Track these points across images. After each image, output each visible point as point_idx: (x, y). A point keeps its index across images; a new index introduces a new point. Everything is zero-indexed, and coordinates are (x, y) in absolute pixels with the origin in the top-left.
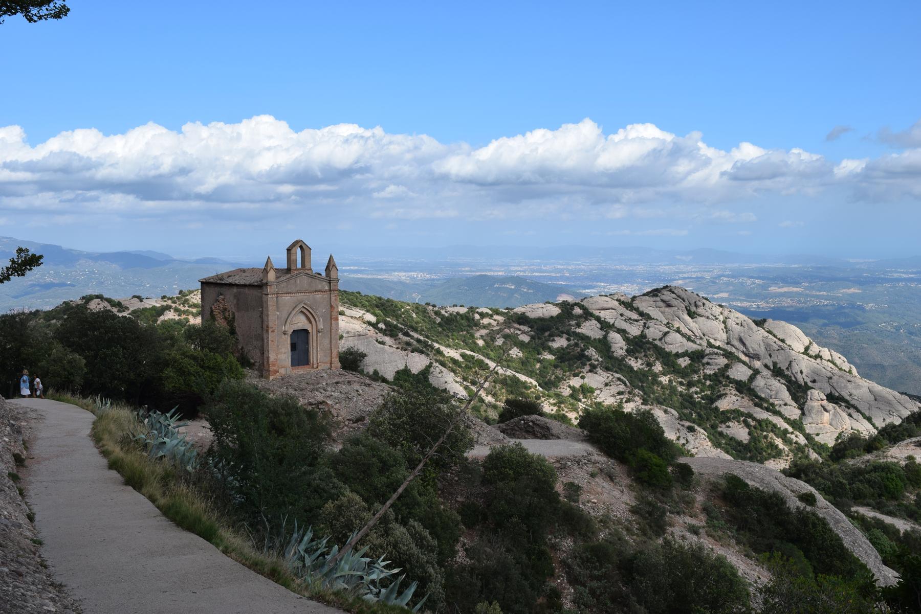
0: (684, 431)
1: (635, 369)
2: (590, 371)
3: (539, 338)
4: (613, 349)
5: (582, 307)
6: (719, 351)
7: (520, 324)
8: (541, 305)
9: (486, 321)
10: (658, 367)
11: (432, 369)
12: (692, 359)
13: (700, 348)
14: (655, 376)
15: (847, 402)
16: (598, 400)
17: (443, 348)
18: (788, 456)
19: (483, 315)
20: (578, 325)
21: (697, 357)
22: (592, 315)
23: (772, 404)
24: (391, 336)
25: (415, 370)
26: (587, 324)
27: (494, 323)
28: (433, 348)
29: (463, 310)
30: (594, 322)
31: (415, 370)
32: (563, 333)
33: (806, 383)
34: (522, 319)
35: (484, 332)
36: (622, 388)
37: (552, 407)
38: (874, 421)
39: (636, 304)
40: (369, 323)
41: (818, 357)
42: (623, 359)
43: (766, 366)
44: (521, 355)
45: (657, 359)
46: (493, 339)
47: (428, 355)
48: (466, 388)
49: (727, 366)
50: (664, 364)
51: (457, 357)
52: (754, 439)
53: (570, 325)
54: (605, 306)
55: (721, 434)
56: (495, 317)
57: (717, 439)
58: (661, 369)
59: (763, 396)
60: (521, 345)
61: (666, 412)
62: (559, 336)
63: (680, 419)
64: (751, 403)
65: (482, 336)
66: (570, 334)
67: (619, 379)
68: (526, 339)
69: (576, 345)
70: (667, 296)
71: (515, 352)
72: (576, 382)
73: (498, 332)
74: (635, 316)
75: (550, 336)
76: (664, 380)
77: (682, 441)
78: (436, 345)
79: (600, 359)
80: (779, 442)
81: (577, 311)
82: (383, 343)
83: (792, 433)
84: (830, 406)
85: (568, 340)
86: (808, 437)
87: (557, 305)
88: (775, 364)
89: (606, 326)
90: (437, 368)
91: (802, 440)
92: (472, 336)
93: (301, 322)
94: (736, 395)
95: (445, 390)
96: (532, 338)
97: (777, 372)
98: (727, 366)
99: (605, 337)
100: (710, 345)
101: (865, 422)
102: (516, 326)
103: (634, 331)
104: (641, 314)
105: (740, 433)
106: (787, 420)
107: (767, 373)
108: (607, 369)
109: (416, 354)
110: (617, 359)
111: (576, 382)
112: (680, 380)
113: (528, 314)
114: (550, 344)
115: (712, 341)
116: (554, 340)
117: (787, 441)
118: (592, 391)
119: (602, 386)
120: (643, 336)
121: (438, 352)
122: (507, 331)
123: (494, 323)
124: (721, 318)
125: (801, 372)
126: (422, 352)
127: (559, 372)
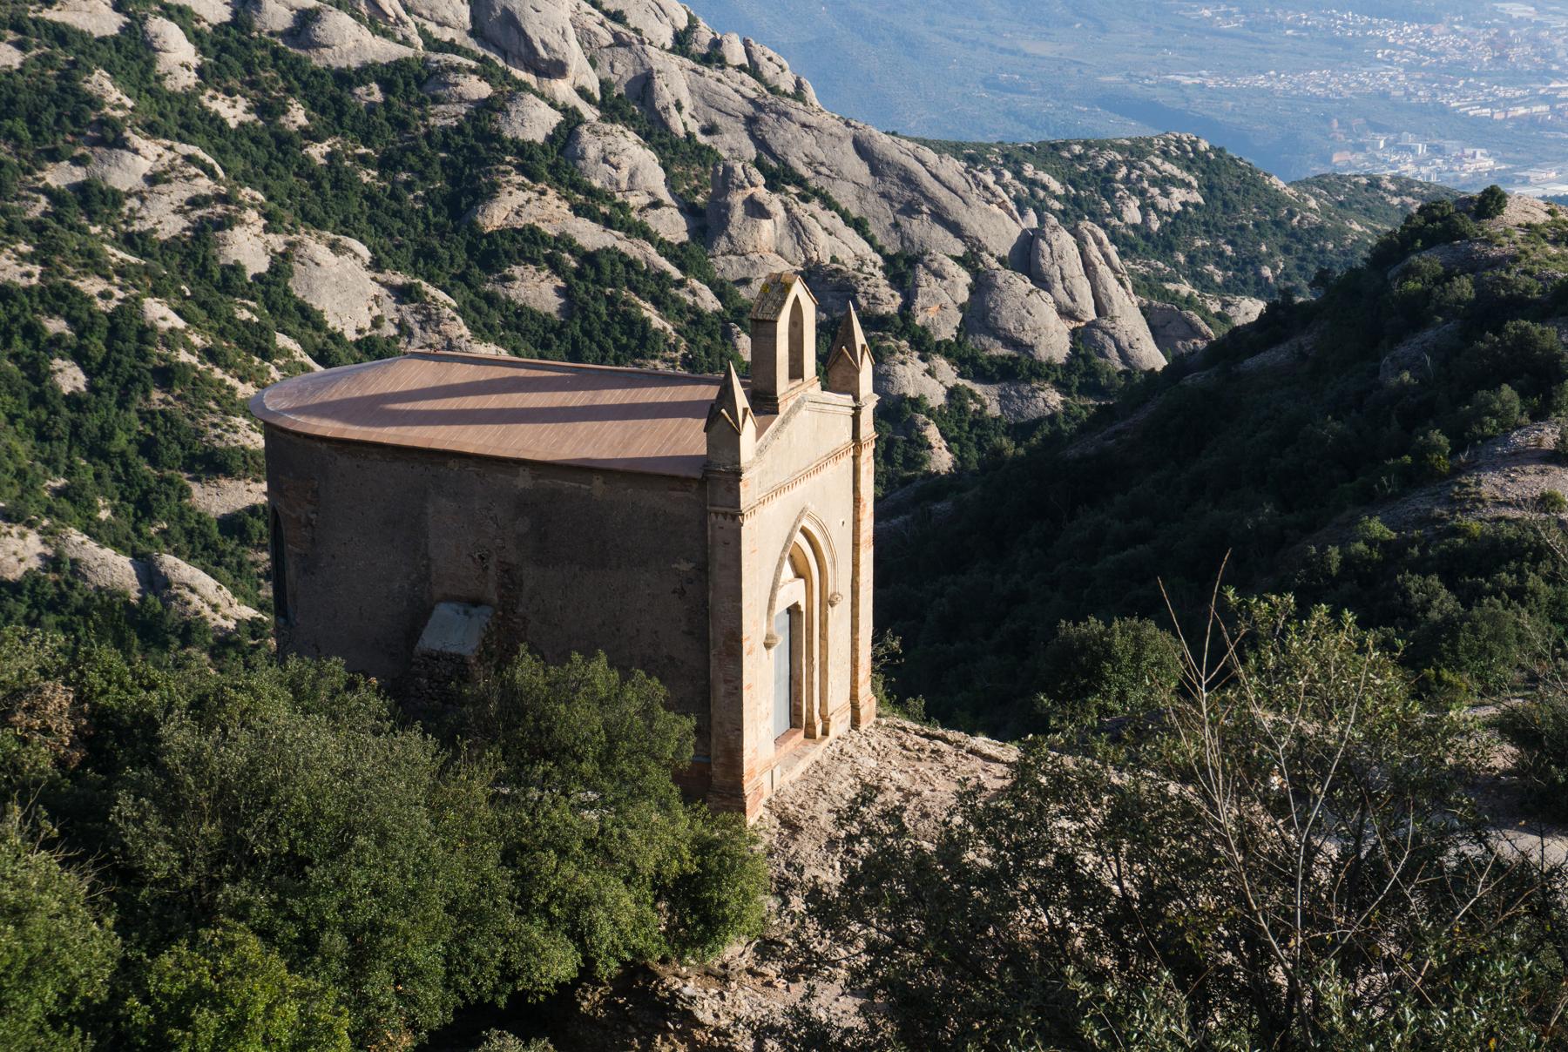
1: (233, 124)
4: (161, 68)
6: (465, 61)
10: (297, 116)
12: (387, 87)
13: (407, 52)
14: (284, 141)
15: (800, 182)
16: (137, 226)
18: (675, 348)
23: (623, 207)
33: (690, 136)
37: (28, 267)
38: (873, 230)
43: (582, 92)
45: (290, 91)
50: (312, 105)
55: (491, 299)
58: (302, 120)
59: (597, 184)
61: (334, 247)
63: (376, 265)
64: (565, 206)
67: (189, 159)
69: (45, 61)
79: (129, 103)
83: (680, 284)
84: (774, 203)
85: (21, 46)
86: (721, 290)
88: (605, 85)
91: (709, 302)
93: (793, 591)
94: (522, 187)
97: (611, 108)
100: (433, 44)
101: (849, 234)
105: (536, 290)
106: (663, 247)
107: (590, 113)
108: (152, 130)
110: (172, 97)
112: (363, 150)
115: (431, 27)
118: (115, 198)
119: (143, 185)
125: (679, 106)
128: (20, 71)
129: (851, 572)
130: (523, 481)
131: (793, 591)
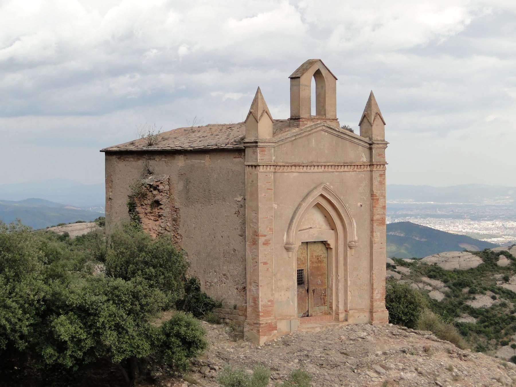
3: (456, 296)
5: (509, 256)
7: (430, 277)
20: (506, 279)
32: (485, 289)
34: (434, 272)
53: (495, 280)
56: (399, 268)
62: (482, 293)
68: (438, 296)
69: (504, 305)
81: (503, 261)
85: (494, 298)
87: (475, 254)
96: (447, 295)
102: (425, 279)
113: (441, 265)
114: (469, 303)
116: (474, 298)
123: (398, 276)
128: (492, 308)
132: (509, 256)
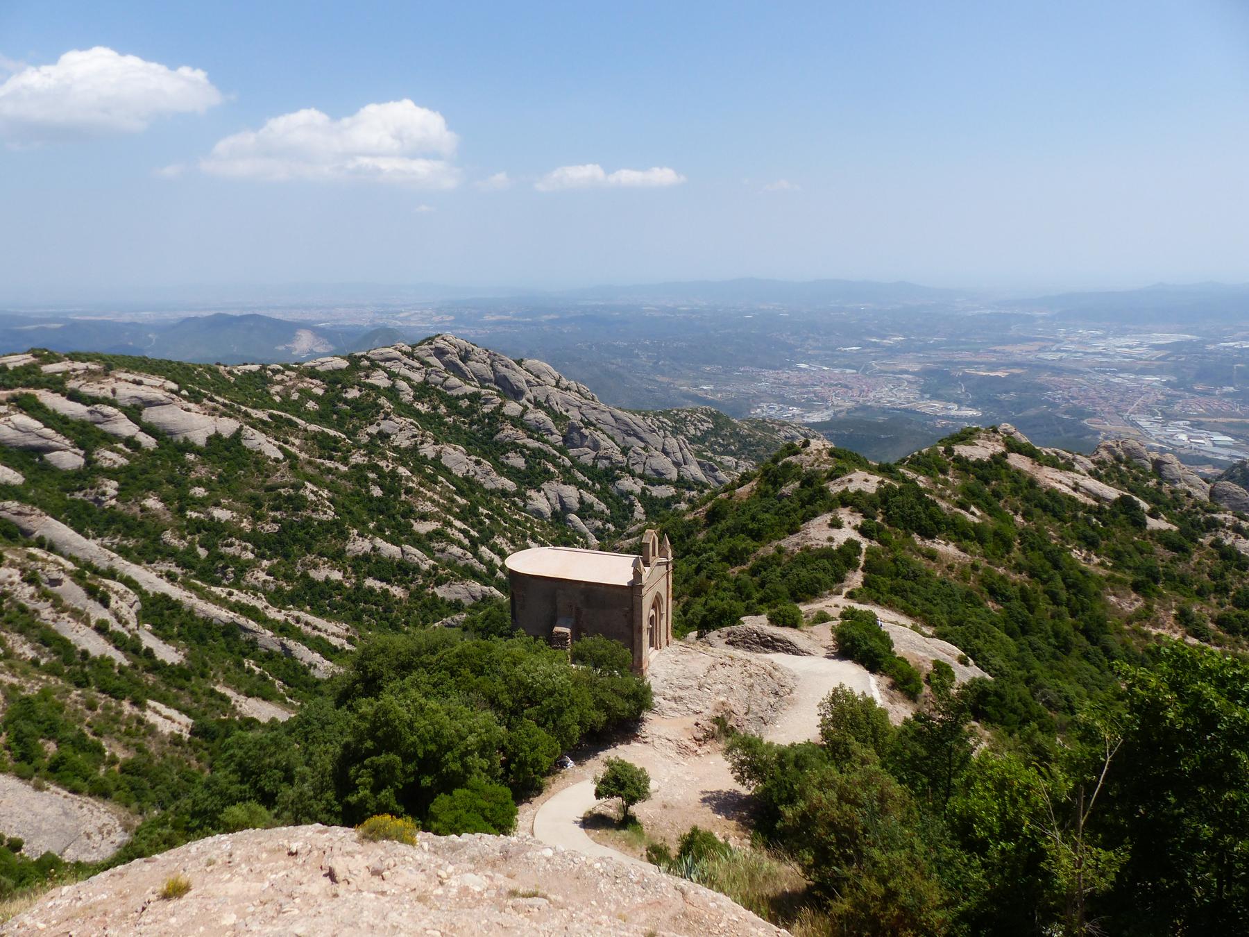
0: (472, 465)
2: (385, 419)
5: (368, 359)
8: (329, 359)
9: (278, 377)
10: (443, 410)
11: (243, 432)
14: (440, 417)
17: (250, 410)
19: (275, 372)
20: (367, 377)
21: (474, 397)
22: (379, 367)
24: (197, 403)
25: (226, 435)
26: (375, 374)
27: (287, 379)
28: (239, 411)
29: (255, 368)
30: (381, 372)
31: (226, 435)
34: (313, 373)
35: (278, 388)
36: (415, 431)
39: (418, 353)
40: (172, 391)
41: (567, 389)
42: (412, 405)
43: (529, 401)
44: (317, 407)
46: (289, 395)
47: (237, 419)
48: (280, 448)
49: (502, 405)
50: (447, 407)
51: (266, 418)
52: (530, 468)
54: (389, 356)
55: (503, 464)
57: (504, 470)
60: (317, 398)
61: (455, 449)
65: (278, 393)
66: (361, 386)
68: (320, 392)
69: (368, 395)
70: (440, 344)
71: (311, 405)
72: (373, 430)
73: (292, 387)
74: (417, 365)
75: (343, 388)
76: (449, 420)
77: (472, 473)
78: (244, 408)
80: (550, 466)
82: (188, 410)
88: (535, 398)
89: (392, 376)
90: (249, 431)
91: (568, 463)
92: (268, 393)
95: (260, 452)
96: (326, 391)
97: (538, 405)
98: (502, 405)
99: (393, 386)
103: (418, 377)
104: (423, 363)
105: (518, 461)
107: (530, 406)
108: (400, 416)
109: (225, 419)
110: (406, 405)
111: (373, 430)
117: (556, 465)
118: (388, 436)
120: (426, 382)
121: (247, 415)
122: (300, 385)
124: (488, 361)
126: (230, 417)
127: (355, 421)
129: (668, 606)
130: (583, 586)
131: (653, 612)
132: (368, 359)
